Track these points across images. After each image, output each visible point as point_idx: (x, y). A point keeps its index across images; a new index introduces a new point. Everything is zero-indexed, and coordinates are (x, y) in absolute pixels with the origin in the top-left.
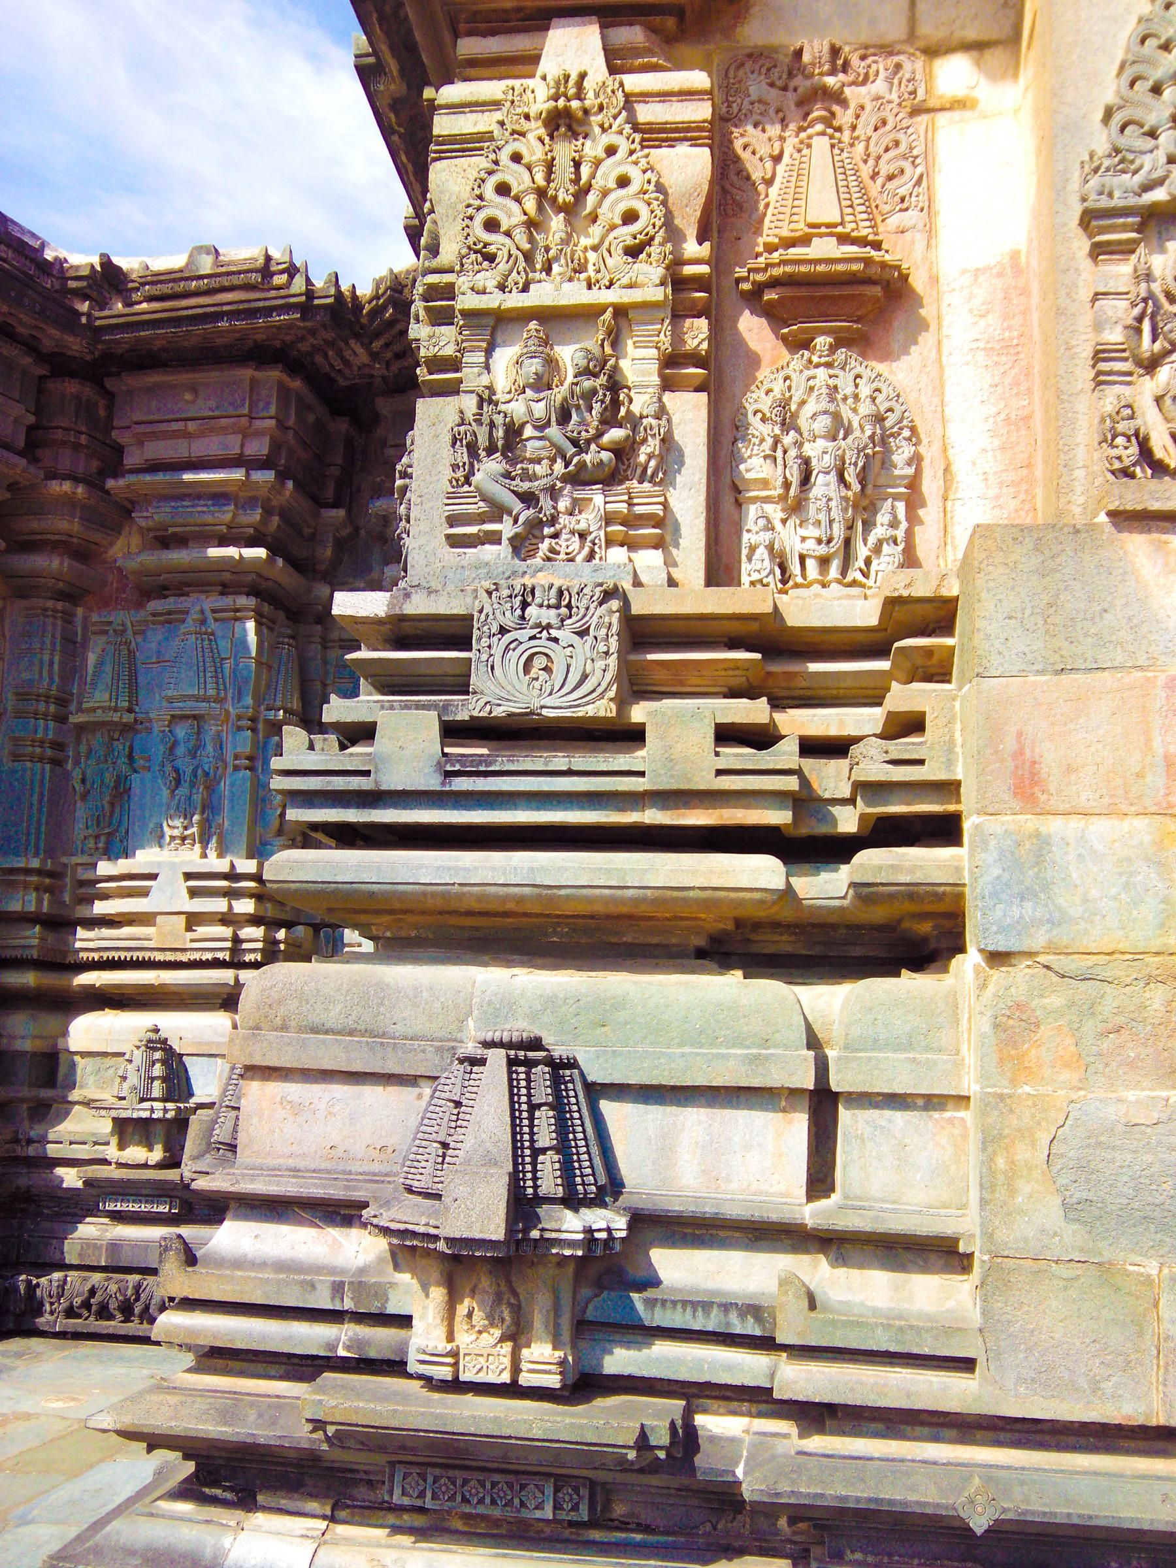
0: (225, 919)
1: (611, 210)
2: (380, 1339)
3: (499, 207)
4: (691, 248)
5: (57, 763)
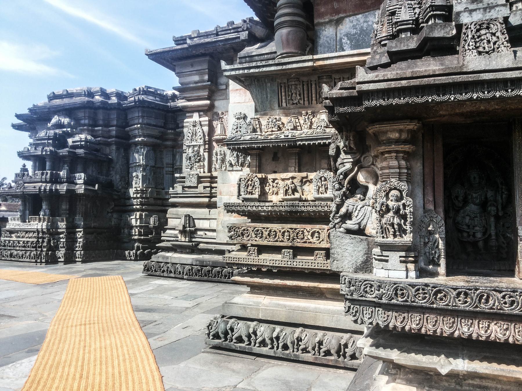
1: (198, 135)
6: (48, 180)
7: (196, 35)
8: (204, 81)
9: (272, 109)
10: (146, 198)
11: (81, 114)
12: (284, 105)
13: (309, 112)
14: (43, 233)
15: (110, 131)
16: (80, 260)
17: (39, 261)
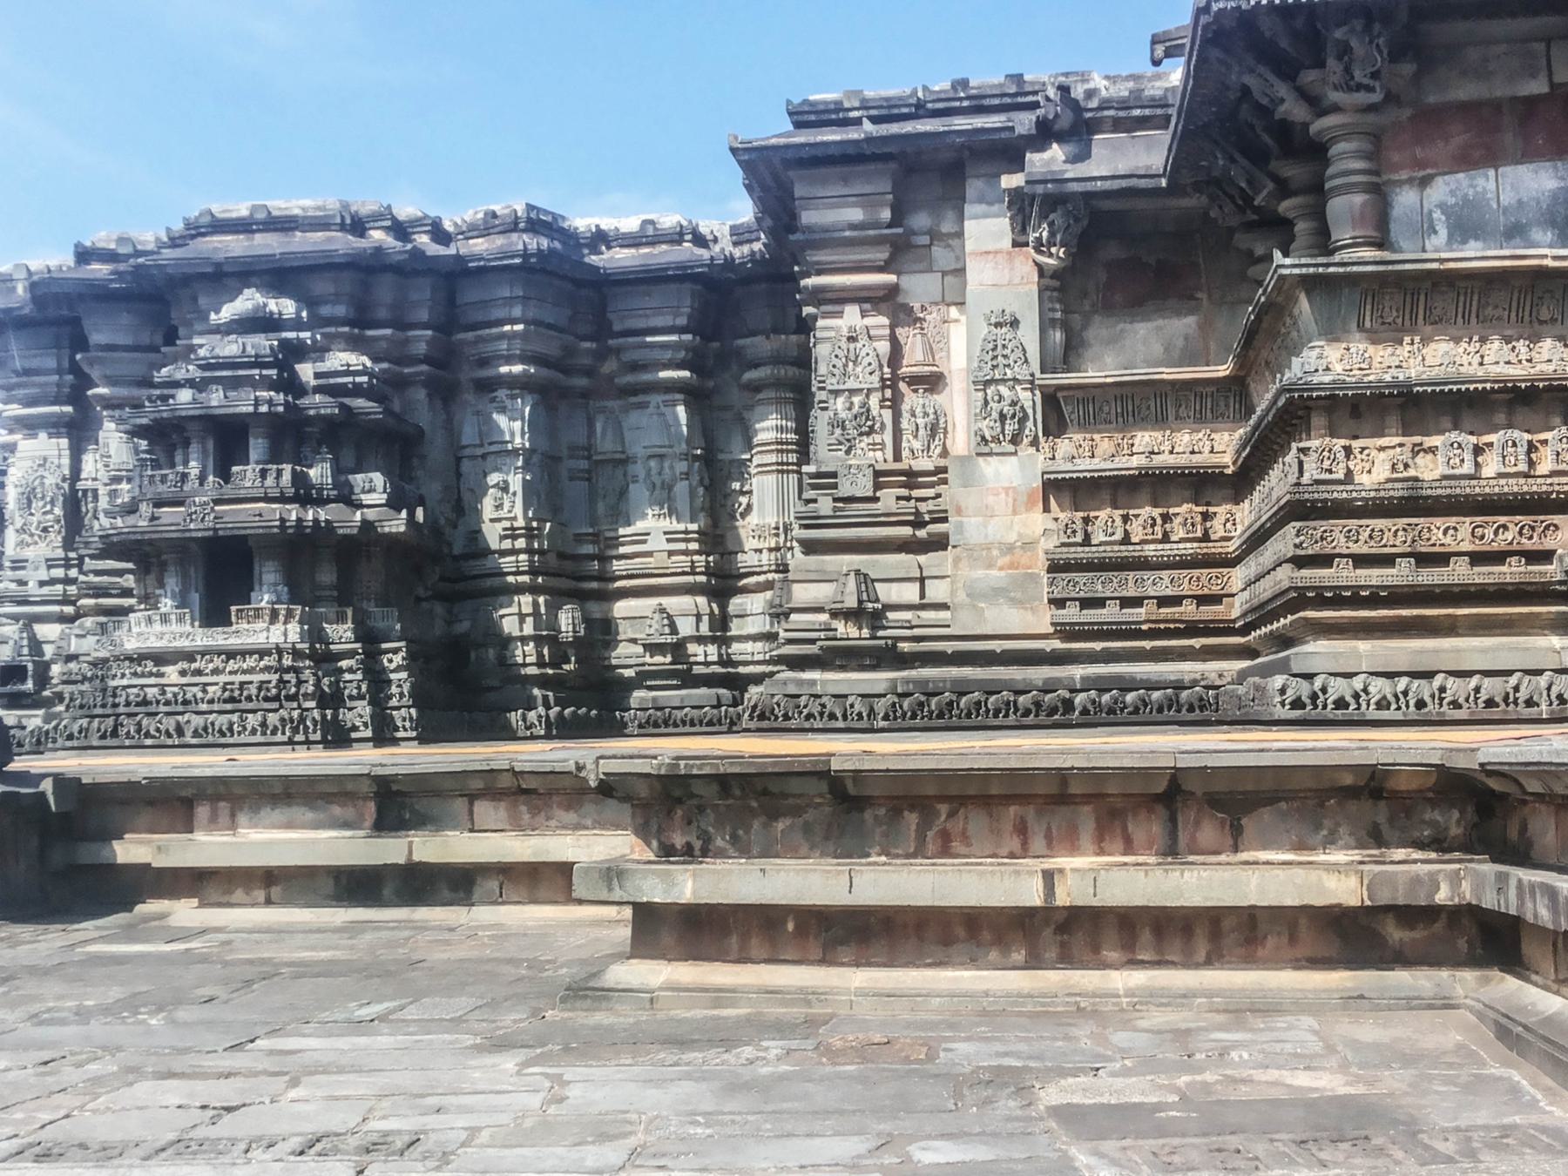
0: (685, 553)
2: (831, 634)
3: (835, 361)
4: (886, 370)
5: (589, 480)
6: (290, 492)
7: (857, 104)
8: (876, 225)
9: (1348, 332)
10: (541, 552)
11: (321, 286)
12: (1368, 324)
13: (1417, 339)
14: (297, 654)
15: (407, 341)
16: (414, 734)
17: (300, 737)
